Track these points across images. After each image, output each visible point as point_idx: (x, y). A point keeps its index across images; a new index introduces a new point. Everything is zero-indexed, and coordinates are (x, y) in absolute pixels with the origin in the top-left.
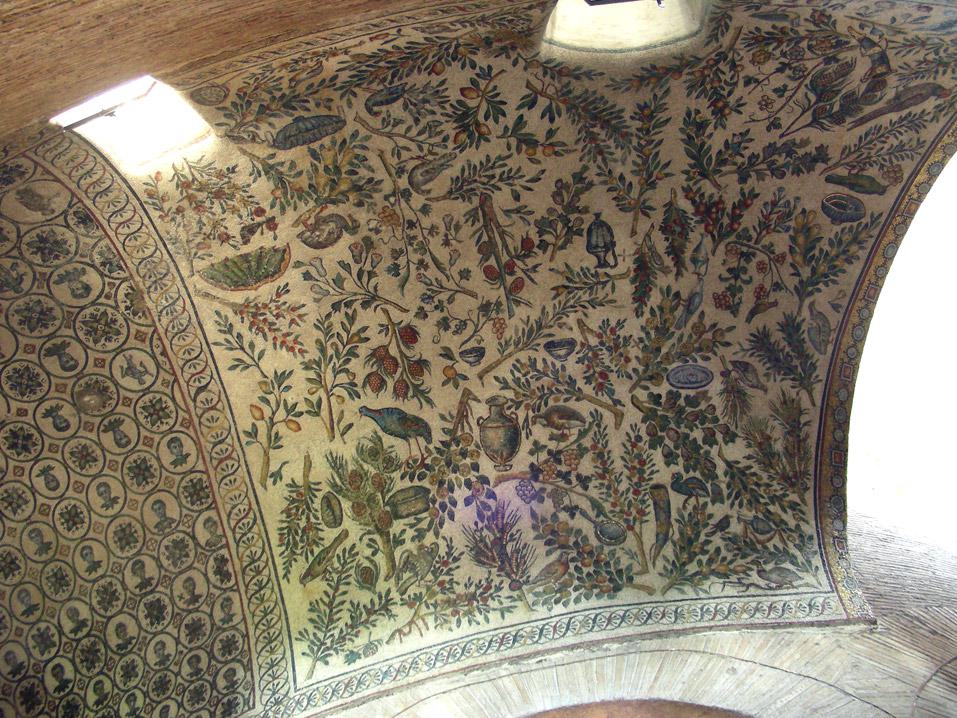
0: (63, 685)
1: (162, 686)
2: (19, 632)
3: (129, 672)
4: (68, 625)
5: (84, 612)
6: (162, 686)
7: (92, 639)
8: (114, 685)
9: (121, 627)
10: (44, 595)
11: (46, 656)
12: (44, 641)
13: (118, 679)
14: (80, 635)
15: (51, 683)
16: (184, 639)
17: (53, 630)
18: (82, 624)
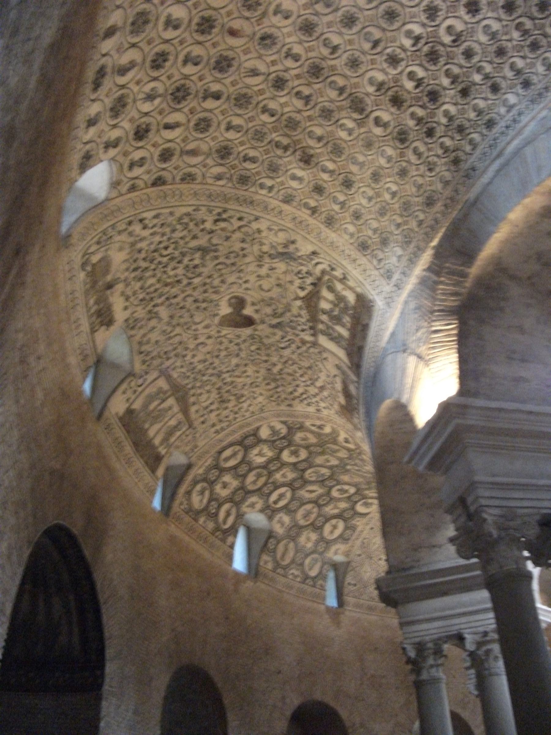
0: (419, 83)
1: (501, 52)
2: (373, 62)
3: (468, 54)
4: (407, 43)
5: (417, 29)
6: (501, 52)
7: (430, 45)
8: (461, 67)
9: (450, 29)
10: (384, 30)
11: (400, 69)
12: (393, 60)
13: (463, 62)
14: (420, 45)
15: (409, 85)
16: (503, 16)
17: (398, 51)
18: (417, 39)
